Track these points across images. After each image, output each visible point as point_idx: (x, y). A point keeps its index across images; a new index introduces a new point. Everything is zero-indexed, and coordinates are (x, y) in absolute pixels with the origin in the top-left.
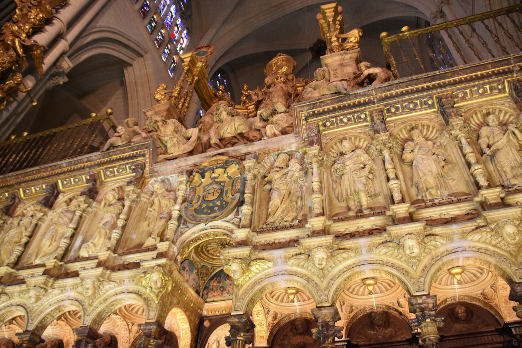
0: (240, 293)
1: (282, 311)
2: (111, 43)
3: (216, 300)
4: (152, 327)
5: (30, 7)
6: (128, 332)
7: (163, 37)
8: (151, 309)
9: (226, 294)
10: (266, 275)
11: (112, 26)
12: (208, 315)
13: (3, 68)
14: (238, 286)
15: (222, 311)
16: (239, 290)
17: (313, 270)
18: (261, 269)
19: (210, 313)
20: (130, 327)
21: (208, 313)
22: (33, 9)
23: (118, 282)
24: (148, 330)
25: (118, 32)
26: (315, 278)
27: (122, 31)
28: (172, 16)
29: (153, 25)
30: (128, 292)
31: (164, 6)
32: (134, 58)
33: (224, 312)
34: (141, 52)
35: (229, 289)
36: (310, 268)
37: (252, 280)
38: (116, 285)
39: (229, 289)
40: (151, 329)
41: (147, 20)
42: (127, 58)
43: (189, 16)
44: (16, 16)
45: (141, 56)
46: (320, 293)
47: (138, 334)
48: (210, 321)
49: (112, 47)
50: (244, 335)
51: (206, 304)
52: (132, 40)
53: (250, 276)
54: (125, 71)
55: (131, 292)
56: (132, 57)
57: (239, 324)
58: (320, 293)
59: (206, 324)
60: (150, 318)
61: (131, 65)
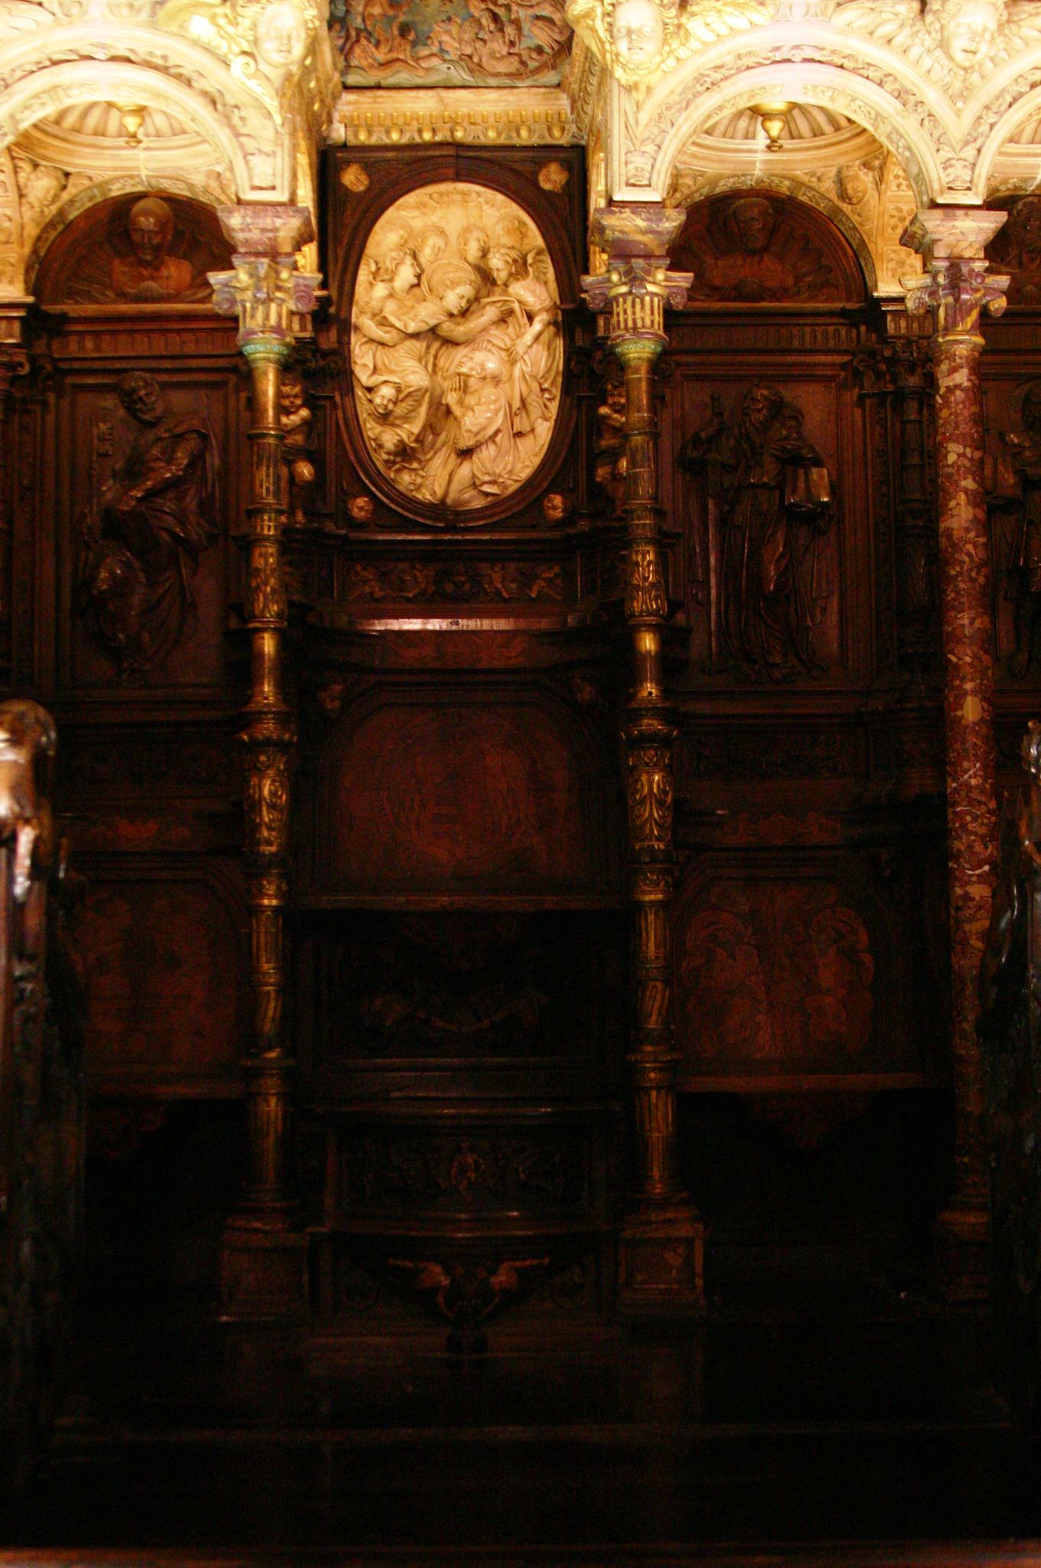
0: (644, 117)
1: (697, 165)
3: (391, 81)
4: (278, 222)
6: (13, 195)
8: (250, 145)
9: (435, 62)
10: (739, 57)
12: (352, 141)
14: (630, 89)
15: (420, 131)
16: (638, 106)
17: (927, 62)
18: (723, 31)
19: (363, 137)
20: (22, 175)
21: (356, 136)
23: (56, 9)
24: (264, 230)
26: (933, 98)
30: (113, 59)
33: (427, 136)
35: (445, 38)
36: (915, 52)
37: (688, 72)
38: (47, 18)
39: (445, 38)
40: (275, 230)
46: (946, 153)
47: (54, 209)
48: (368, 167)
50: (666, 280)
51: (349, 97)
53: (682, 53)
55: (129, 60)
57: (645, 238)
58: (946, 153)
59: (353, 178)
60: (257, 182)
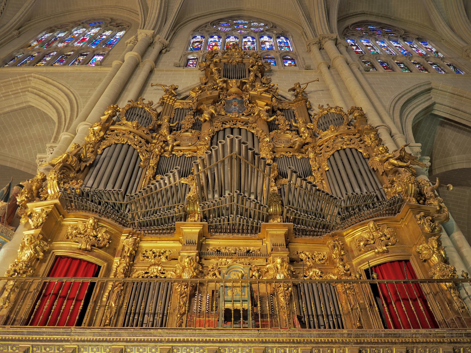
2: (407, 108)
5: (361, 141)
7: (418, 64)
11: (393, 97)
13: (414, 183)
22: (364, 138)
25: (400, 96)
27: (400, 92)
28: (399, 47)
29: (402, 66)
31: (388, 50)
32: (430, 97)
34: (427, 87)
41: (397, 68)
42: (426, 103)
43: (405, 32)
44: (364, 154)
45: (429, 90)
49: (410, 109)
52: (412, 88)
54: (436, 113)
56: (428, 98)
61: (434, 103)
